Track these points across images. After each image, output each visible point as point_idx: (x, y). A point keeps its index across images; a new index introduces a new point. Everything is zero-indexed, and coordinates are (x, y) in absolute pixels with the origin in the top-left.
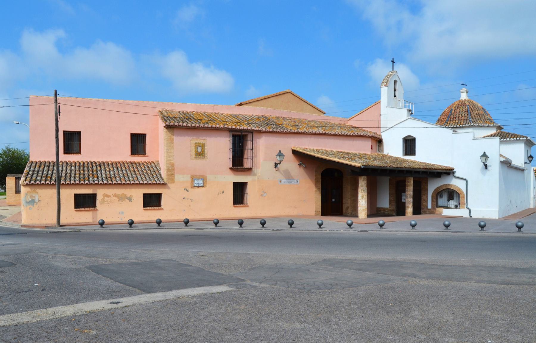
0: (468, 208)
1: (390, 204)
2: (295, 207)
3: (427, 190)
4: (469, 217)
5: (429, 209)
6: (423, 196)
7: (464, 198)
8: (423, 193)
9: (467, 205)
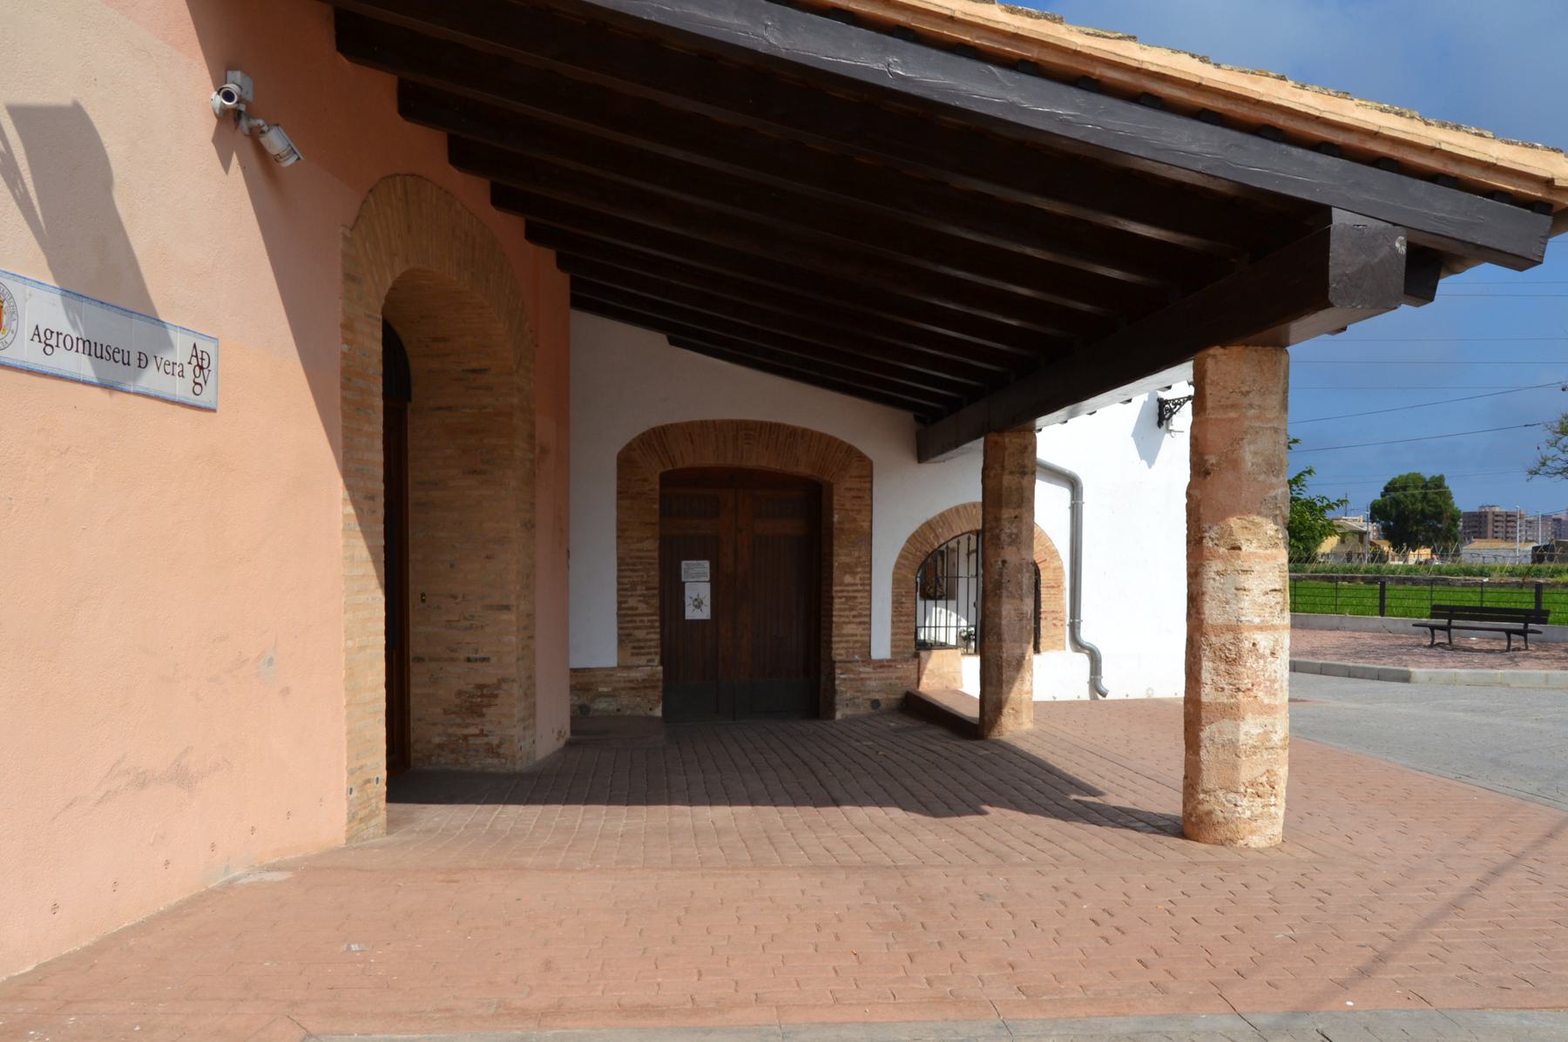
0: (1078, 645)
1: (624, 638)
2: (182, 777)
3: (865, 539)
4: (1084, 694)
5: (881, 665)
6: (843, 582)
7: (1058, 586)
8: (841, 557)
9: (1074, 628)
